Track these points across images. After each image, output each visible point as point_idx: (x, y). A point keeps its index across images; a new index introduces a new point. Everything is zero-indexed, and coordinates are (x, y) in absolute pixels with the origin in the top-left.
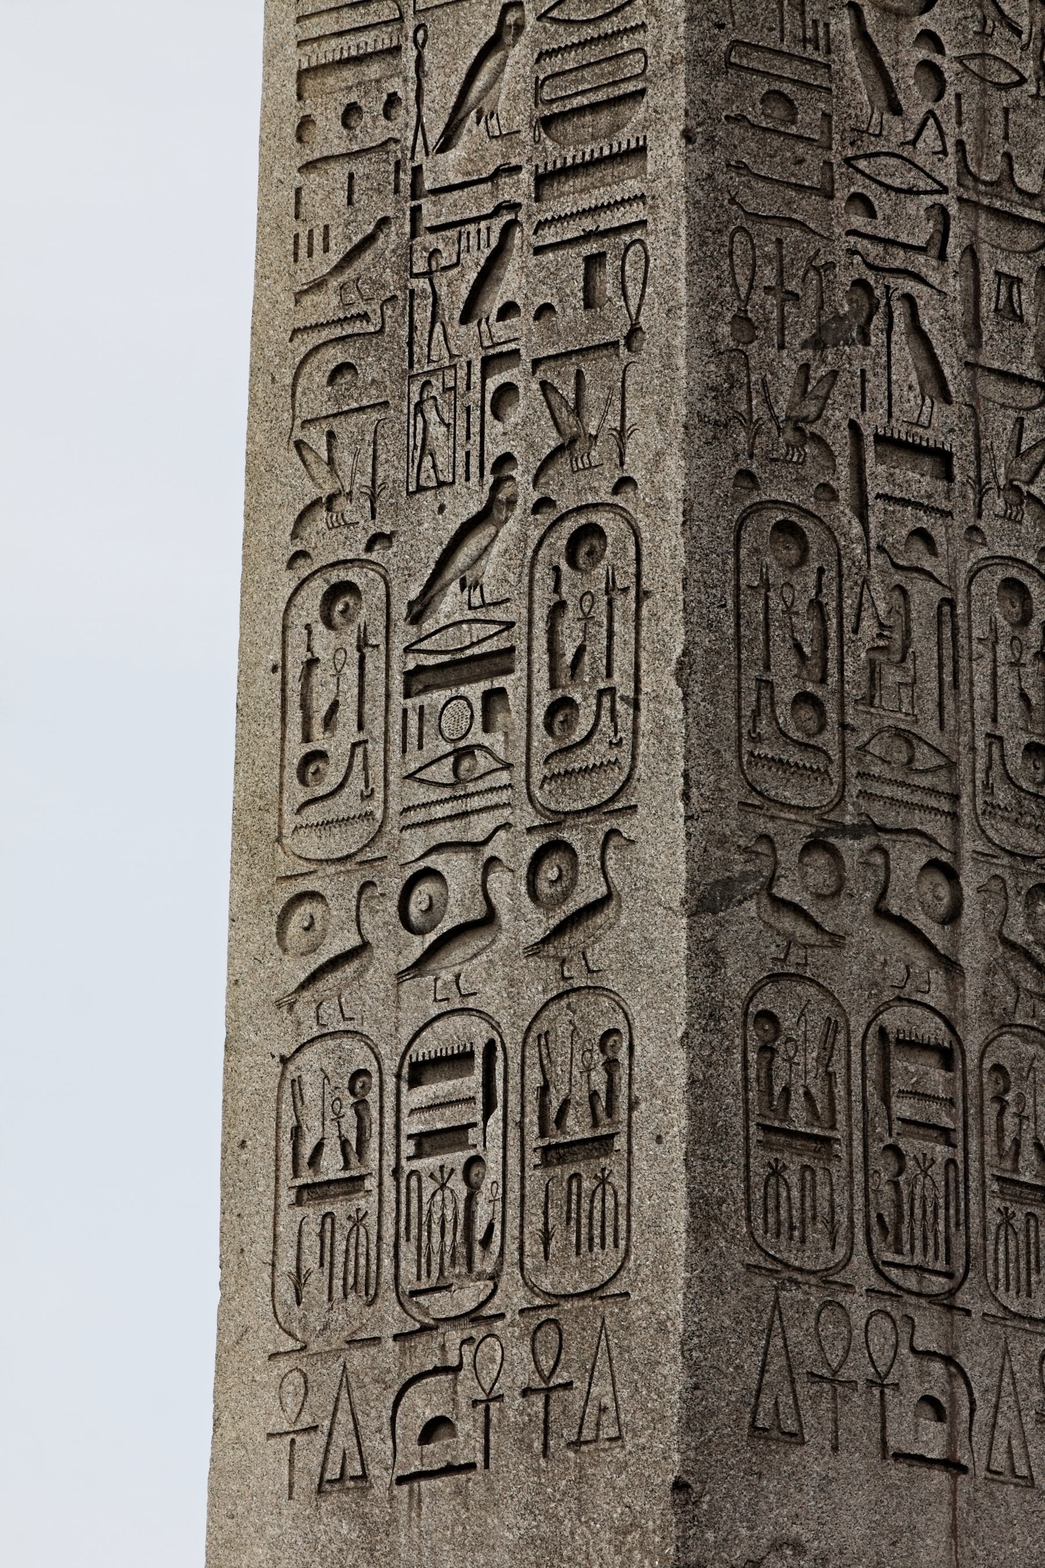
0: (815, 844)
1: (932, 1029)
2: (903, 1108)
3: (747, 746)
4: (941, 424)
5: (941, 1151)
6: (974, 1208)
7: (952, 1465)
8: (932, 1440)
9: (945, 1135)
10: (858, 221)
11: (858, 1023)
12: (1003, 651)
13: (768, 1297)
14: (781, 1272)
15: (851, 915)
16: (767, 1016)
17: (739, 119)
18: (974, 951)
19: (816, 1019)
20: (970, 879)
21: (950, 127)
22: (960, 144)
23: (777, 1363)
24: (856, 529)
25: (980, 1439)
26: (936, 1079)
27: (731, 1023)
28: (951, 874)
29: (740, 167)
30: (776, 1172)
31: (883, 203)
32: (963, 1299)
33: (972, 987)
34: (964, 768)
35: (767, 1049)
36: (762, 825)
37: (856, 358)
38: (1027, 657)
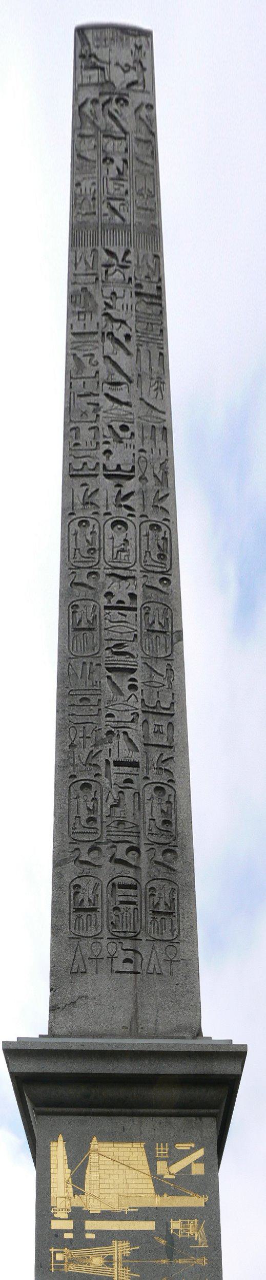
2: (121, 899)
3: (72, 831)
4: (135, 757)
5: (132, 906)
6: (143, 917)
7: (136, 973)
8: (129, 967)
9: (134, 903)
10: (108, 719)
11: (105, 883)
12: (155, 801)
13: (76, 944)
14: (80, 937)
15: (105, 861)
16: (78, 886)
17: (73, 705)
18: (144, 864)
19: (92, 884)
20: (143, 849)
21: (140, 697)
22: (143, 700)
23: (79, 957)
24: (107, 781)
25: (145, 966)
26: (131, 892)
27: (66, 889)
28: (137, 850)
29: (73, 715)
30: (79, 917)
32: (138, 937)
33: (144, 872)
34: (142, 826)
35: (76, 893)
36: (76, 846)
37: (108, 746)
38: (164, 802)
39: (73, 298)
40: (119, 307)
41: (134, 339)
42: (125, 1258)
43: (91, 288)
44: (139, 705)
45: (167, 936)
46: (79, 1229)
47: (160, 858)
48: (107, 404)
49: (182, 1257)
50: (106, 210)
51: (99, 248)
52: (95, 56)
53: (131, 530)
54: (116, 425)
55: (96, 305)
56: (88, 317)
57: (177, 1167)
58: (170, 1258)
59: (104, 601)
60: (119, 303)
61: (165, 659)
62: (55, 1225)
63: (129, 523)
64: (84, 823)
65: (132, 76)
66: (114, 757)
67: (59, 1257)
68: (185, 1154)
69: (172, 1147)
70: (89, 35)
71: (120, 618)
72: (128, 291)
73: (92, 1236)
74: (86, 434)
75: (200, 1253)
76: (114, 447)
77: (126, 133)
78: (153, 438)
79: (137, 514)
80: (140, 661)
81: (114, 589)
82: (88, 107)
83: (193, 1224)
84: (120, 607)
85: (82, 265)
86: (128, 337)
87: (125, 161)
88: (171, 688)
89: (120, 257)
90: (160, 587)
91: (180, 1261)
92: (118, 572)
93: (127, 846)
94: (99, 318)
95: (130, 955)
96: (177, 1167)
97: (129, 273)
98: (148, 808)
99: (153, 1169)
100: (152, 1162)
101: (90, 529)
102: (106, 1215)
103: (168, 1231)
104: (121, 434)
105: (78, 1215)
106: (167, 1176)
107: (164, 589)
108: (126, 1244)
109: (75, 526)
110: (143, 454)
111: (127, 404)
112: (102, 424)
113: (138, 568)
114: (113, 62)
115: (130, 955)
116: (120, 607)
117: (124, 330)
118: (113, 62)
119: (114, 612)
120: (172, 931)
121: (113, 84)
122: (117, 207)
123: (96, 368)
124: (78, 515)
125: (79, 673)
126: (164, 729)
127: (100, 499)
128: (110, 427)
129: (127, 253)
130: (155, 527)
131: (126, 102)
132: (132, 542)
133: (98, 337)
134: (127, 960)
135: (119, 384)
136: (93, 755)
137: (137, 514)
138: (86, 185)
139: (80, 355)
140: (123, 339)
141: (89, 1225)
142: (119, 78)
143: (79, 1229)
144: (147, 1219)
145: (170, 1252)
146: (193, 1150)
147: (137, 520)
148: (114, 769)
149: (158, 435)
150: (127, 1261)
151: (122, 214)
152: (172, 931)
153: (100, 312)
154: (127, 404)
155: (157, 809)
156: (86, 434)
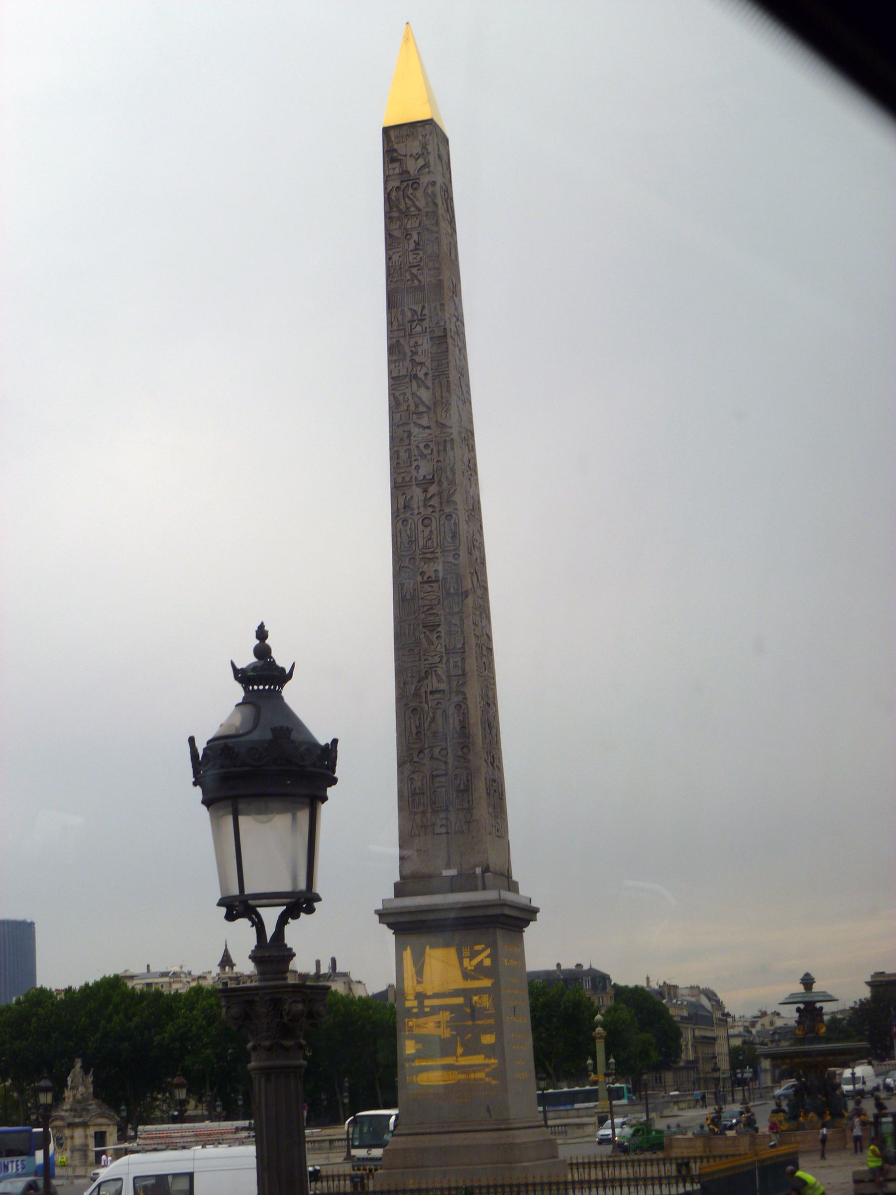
0: (420, 752)
1: (444, 772)
4: (443, 686)
5: (444, 789)
7: (447, 833)
8: (443, 830)
14: (416, 813)
15: (426, 761)
18: (450, 759)
20: (449, 750)
26: (443, 779)
28: (446, 749)
31: (430, 658)
33: (450, 766)
35: (412, 783)
37: (426, 682)
39: (391, 349)
40: (420, 353)
41: (430, 375)
43: (402, 340)
44: (443, 650)
45: (465, 805)
46: (421, 1005)
47: (460, 753)
48: (415, 431)
50: (409, 277)
51: (406, 309)
52: (396, 151)
53: (434, 524)
54: (422, 446)
55: (405, 355)
56: (401, 364)
57: (475, 961)
58: (473, 1020)
59: (419, 579)
60: (420, 349)
61: (458, 613)
62: (408, 1004)
63: (433, 519)
64: (414, 736)
65: (421, 162)
66: (430, 689)
67: (410, 1024)
68: (479, 952)
69: (472, 948)
70: (392, 134)
71: (429, 589)
72: (425, 341)
74: (404, 455)
75: (489, 1016)
76: (422, 463)
77: (419, 210)
78: (445, 450)
79: (437, 511)
80: (442, 618)
81: (425, 568)
82: (394, 194)
84: (429, 581)
85: (395, 323)
86: (426, 374)
87: (419, 233)
88: (463, 632)
90: (453, 561)
91: (479, 1022)
92: (428, 556)
93: (439, 749)
94: (408, 364)
95: (444, 822)
96: (475, 961)
97: (426, 324)
98: (451, 721)
99: (461, 963)
100: (461, 959)
101: (409, 526)
103: (471, 1004)
104: (426, 452)
105: (420, 997)
106: (469, 968)
107: (456, 562)
108: (448, 1013)
109: (400, 524)
110: (439, 464)
111: (428, 428)
112: (413, 447)
113: (438, 550)
114: (409, 154)
115: (444, 822)
116: (429, 581)
117: (424, 370)
118: (409, 154)
119: (426, 586)
120: (469, 802)
121: (408, 172)
122: (415, 272)
123: (406, 404)
124: (402, 516)
125: (407, 631)
126: (460, 664)
127: (414, 504)
128: (417, 447)
129: (423, 307)
130: (449, 516)
131: (418, 183)
132: (435, 532)
133: (407, 380)
134: (441, 826)
135: (424, 412)
136: (417, 689)
137: (437, 511)
138: (395, 258)
139: (397, 394)
140: (423, 377)
141: (427, 1002)
142: (412, 166)
143: (421, 1005)
144: (459, 996)
145: (473, 1016)
146: (483, 950)
147: (436, 515)
148: (430, 697)
149: (448, 448)
150: (450, 1024)
151: (420, 278)
152: (469, 802)
153: (408, 359)
154: (428, 428)
155: (457, 720)
156: (404, 455)
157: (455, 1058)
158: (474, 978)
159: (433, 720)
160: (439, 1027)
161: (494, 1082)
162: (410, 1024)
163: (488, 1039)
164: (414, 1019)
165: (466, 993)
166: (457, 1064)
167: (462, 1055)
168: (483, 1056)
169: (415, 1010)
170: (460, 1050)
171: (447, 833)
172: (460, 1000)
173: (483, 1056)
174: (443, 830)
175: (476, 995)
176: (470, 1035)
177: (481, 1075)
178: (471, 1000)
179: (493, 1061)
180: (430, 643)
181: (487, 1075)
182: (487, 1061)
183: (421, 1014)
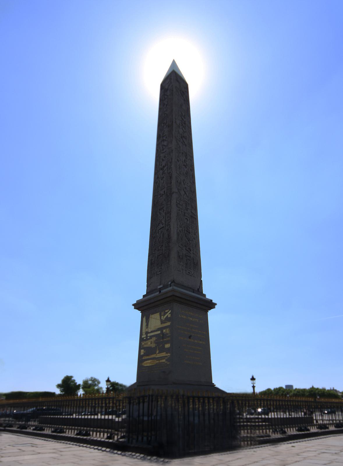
8: (160, 273)
28: (162, 246)
42: (154, 341)
46: (147, 336)
49: (166, 338)
57: (165, 317)
58: (163, 339)
69: (165, 311)
73: (148, 337)
83: (168, 329)
89: (165, 122)
91: (165, 339)
102: (152, 332)
103: (163, 333)
108: (155, 338)
116: (162, 195)
141: (149, 335)
143: (147, 336)
144: (159, 331)
150: (155, 342)
157: (155, 355)
158: (164, 323)
159: (160, 237)
160: (151, 344)
161: (168, 363)
162: (143, 344)
163: (167, 346)
164: (144, 342)
165: (161, 329)
166: (156, 357)
167: (158, 353)
168: (165, 353)
169: (145, 338)
170: (157, 352)
171: (161, 273)
172: (159, 332)
173: (165, 353)
174: (160, 273)
175: (164, 329)
176: (161, 345)
177: (164, 361)
178: (163, 331)
179: (169, 354)
180: (160, 214)
181: (166, 360)
182: (167, 355)
183: (147, 339)
